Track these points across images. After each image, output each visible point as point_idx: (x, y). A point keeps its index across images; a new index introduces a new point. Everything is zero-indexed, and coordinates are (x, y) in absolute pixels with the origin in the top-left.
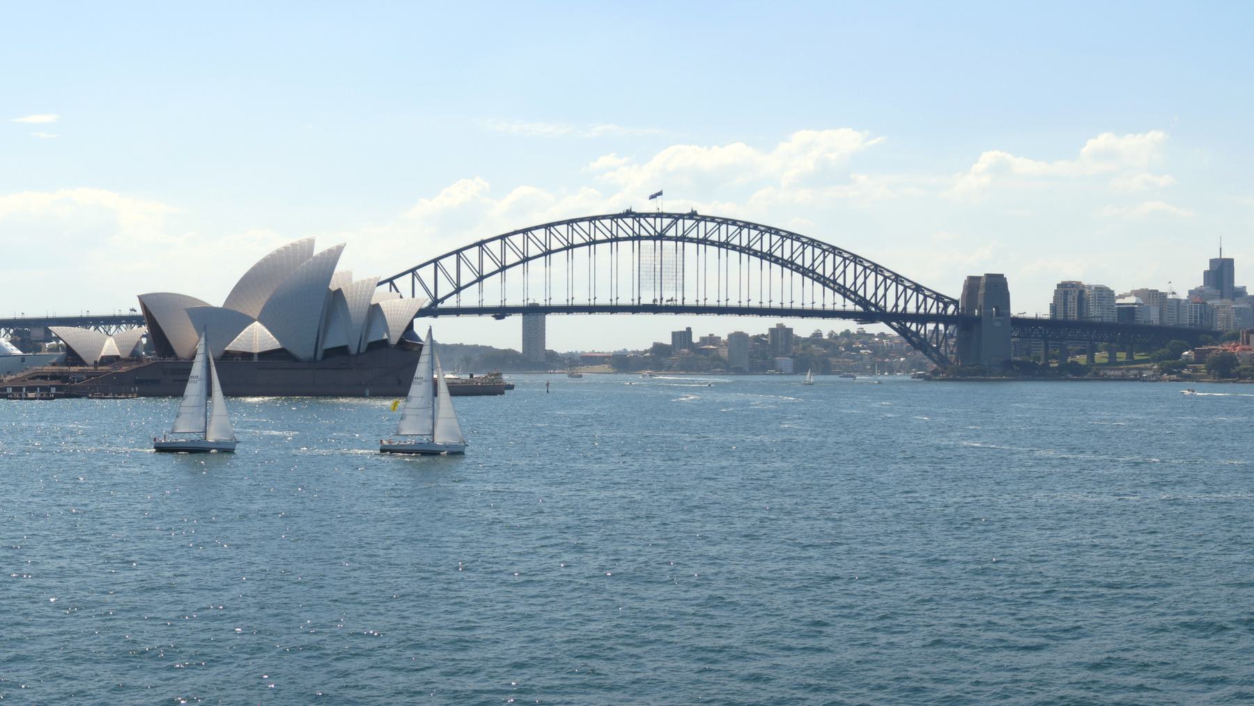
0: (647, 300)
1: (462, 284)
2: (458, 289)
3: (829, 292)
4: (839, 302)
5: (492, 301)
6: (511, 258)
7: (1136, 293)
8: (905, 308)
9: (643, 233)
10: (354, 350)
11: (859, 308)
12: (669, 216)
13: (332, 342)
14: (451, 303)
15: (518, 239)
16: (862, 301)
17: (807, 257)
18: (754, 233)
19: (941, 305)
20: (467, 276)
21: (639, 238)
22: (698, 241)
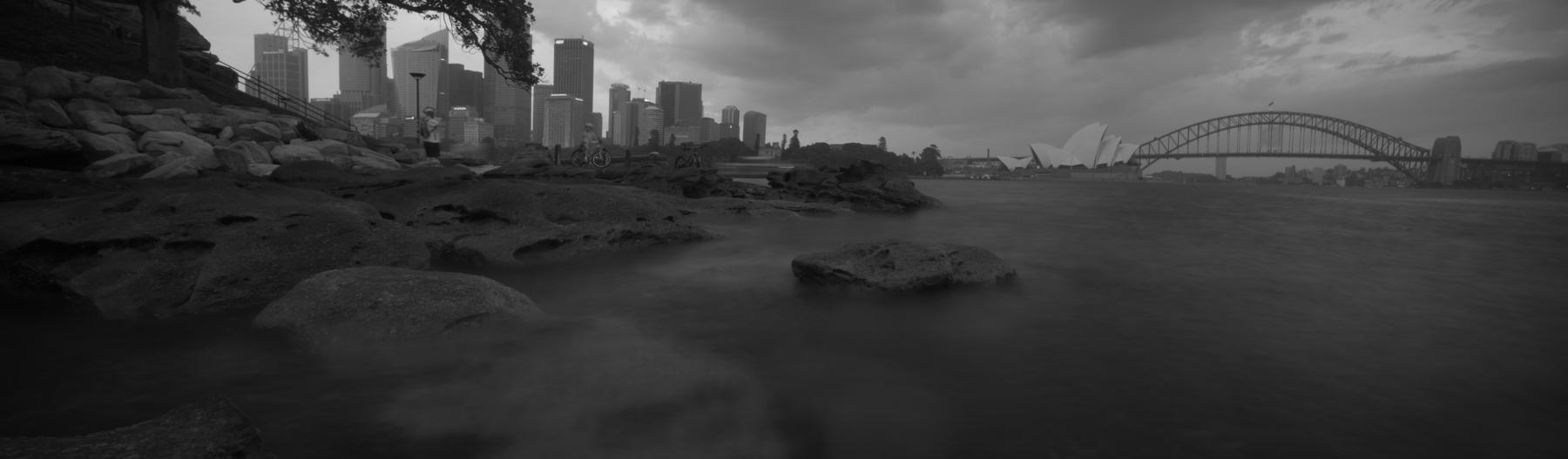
0: (1264, 150)
1: (1180, 143)
2: (1178, 147)
3: (1357, 146)
4: (1362, 151)
5: (1192, 151)
6: (1202, 133)
7: (1554, 146)
8: (1399, 154)
9: (1263, 121)
10: (1109, 165)
11: (1372, 154)
12: (1276, 113)
13: (1100, 162)
14: (1175, 152)
15: (1205, 125)
16: (1374, 151)
17: (1345, 131)
18: (1319, 120)
19: (1419, 153)
20: (1182, 141)
21: (1260, 123)
22: (1291, 124)
